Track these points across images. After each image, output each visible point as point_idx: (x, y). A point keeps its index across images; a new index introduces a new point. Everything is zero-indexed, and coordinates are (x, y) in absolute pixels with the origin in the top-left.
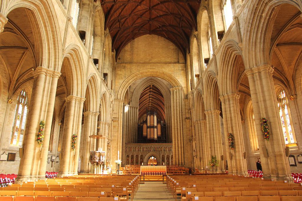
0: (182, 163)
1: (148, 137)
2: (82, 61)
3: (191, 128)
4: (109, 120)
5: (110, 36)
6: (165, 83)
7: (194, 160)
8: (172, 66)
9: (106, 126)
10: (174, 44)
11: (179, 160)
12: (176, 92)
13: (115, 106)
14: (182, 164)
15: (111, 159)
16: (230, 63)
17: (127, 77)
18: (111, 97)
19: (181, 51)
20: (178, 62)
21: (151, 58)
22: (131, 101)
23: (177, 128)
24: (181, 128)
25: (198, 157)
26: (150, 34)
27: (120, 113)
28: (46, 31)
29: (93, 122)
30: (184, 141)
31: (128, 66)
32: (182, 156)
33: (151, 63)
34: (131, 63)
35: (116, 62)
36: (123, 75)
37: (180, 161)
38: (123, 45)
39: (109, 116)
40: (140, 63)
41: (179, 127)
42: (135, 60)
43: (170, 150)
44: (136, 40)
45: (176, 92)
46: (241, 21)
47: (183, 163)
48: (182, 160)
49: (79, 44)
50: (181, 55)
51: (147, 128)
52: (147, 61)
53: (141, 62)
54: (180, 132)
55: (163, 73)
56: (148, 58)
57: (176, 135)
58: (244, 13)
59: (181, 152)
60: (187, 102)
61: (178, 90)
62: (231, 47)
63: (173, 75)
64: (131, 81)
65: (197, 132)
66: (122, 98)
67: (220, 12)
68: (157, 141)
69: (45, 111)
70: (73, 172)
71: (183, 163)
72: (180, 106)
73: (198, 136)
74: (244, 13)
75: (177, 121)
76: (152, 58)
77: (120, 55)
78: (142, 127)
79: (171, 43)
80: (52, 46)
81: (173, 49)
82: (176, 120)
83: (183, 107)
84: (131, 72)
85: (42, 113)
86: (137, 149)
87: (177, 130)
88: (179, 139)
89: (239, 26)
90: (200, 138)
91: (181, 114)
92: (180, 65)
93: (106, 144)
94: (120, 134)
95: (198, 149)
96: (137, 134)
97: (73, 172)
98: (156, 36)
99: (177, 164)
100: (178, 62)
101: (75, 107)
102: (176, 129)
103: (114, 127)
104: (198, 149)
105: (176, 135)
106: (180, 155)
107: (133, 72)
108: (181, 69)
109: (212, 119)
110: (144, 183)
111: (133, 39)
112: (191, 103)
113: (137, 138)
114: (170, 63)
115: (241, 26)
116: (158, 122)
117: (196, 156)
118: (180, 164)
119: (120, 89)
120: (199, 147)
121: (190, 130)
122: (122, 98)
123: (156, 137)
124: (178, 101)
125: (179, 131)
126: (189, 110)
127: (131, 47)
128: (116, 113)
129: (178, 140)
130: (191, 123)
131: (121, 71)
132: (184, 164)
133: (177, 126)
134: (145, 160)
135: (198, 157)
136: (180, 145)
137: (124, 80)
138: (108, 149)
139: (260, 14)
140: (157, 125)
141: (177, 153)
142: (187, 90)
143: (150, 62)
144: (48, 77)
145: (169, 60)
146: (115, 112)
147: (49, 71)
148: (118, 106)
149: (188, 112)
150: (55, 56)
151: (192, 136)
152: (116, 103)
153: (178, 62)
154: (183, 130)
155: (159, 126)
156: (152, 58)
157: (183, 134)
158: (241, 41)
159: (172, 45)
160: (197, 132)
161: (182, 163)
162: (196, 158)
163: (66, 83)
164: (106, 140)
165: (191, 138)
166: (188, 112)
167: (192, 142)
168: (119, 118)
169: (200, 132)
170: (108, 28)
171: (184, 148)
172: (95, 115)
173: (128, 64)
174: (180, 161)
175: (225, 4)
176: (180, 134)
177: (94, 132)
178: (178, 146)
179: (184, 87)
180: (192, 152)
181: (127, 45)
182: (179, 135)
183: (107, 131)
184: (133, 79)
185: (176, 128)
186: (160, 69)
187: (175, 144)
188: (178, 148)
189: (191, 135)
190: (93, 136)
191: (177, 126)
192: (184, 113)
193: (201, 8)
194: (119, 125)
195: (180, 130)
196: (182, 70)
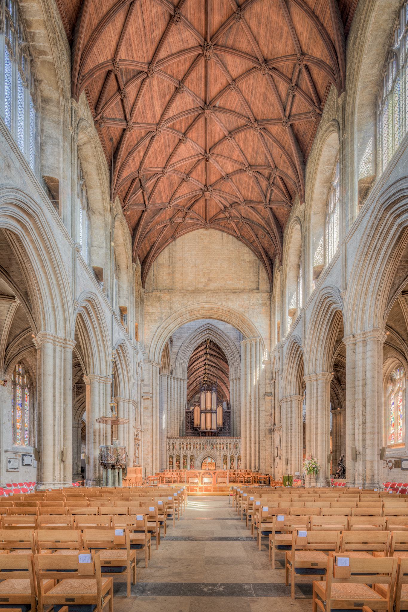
0: (255, 466)
7: (276, 462)
11: (250, 463)
15: (143, 460)
17: (164, 319)
27: (154, 384)
37: (253, 465)
48: (255, 463)
52: (201, 286)
56: (202, 280)
88: (253, 429)
106: (253, 455)
108: (261, 302)
117: (280, 456)
118: (253, 468)
119: (153, 340)
120: (287, 441)
121: (271, 415)
128: (148, 385)
132: (259, 469)
141: (248, 452)
146: (146, 382)
148: (151, 372)
174: (253, 465)
180: (273, 449)
188: (250, 444)
194: (154, 406)
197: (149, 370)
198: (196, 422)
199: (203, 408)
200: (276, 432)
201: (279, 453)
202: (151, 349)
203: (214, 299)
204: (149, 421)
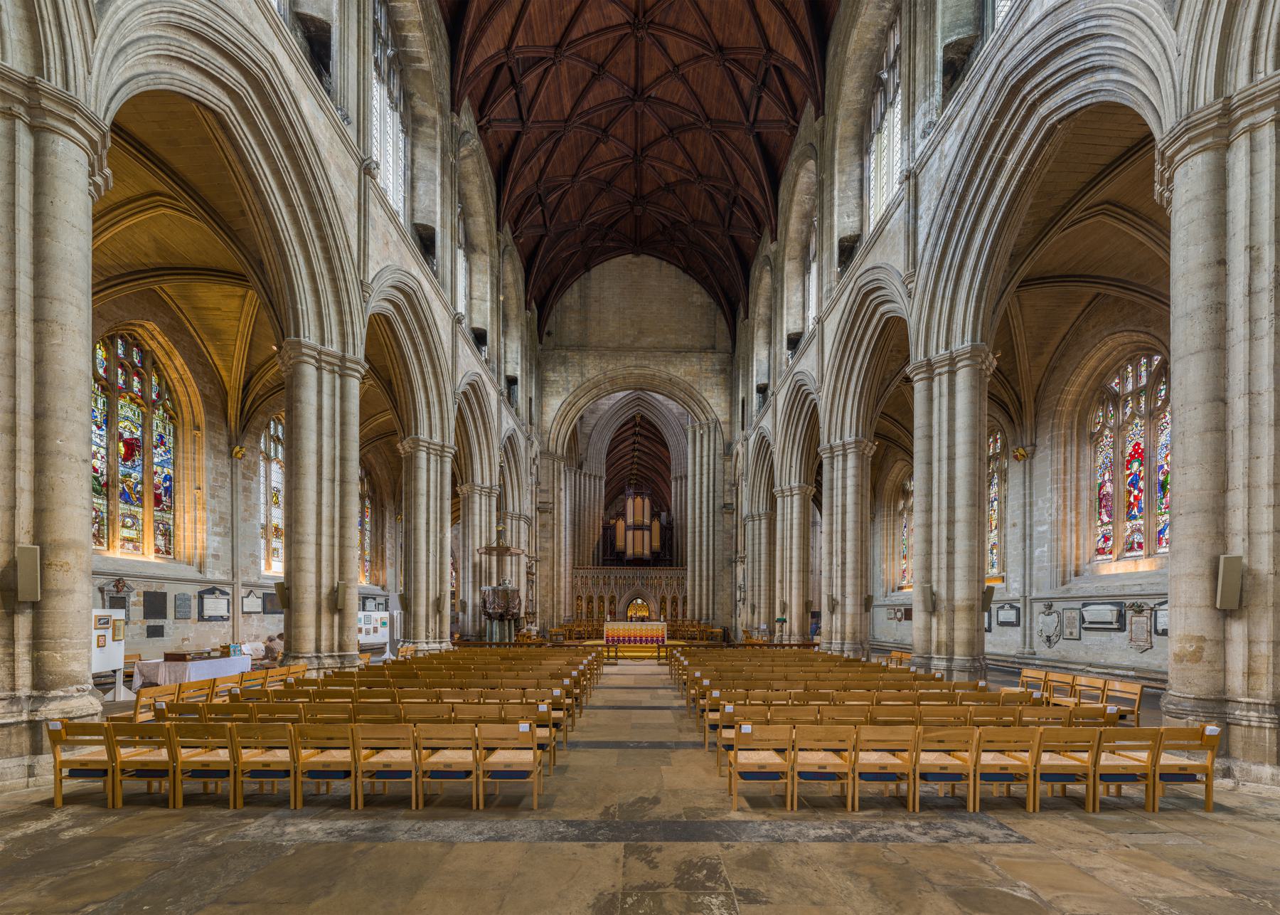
0: (708, 615)
1: (630, 552)
2: (435, 332)
4: (528, 508)
5: (516, 254)
9: (522, 523)
10: (703, 291)
11: (701, 609)
13: (543, 472)
14: (708, 619)
17: (571, 390)
18: (531, 446)
21: (639, 333)
23: (701, 532)
24: (711, 532)
25: (749, 603)
29: (483, 513)
32: (708, 599)
33: (637, 349)
35: (541, 342)
37: (704, 612)
38: (558, 290)
39: (529, 497)
40: (608, 348)
41: (704, 529)
43: (682, 585)
47: (711, 616)
48: (708, 609)
49: (415, 271)
50: (722, 326)
52: (628, 341)
53: (610, 344)
55: (670, 380)
57: (697, 548)
60: (728, 464)
63: (697, 387)
64: (582, 401)
65: (750, 543)
66: (559, 451)
68: (649, 561)
69: (333, 481)
71: (711, 616)
72: (711, 475)
73: (750, 553)
75: (701, 513)
76: (641, 332)
77: (549, 321)
78: (614, 527)
79: (696, 287)
81: (701, 306)
82: (697, 511)
83: (719, 476)
84: (582, 375)
85: (326, 485)
86: (601, 582)
87: (701, 536)
91: (711, 495)
92: (716, 356)
93: (523, 570)
96: (601, 543)
98: (653, 259)
99: (697, 616)
100: (713, 348)
101: (428, 470)
102: (697, 534)
103: (543, 526)
104: (749, 584)
105: (697, 548)
106: (704, 597)
107: (587, 375)
108: (718, 367)
109: (792, 507)
110: (616, 664)
112: (739, 465)
113: (601, 554)
118: (704, 617)
122: (559, 451)
123: (647, 552)
124: (705, 459)
125: (704, 538)
126: (734, 485)
127: (580, 297)
128: (547, 491)
129: (701, 561)
133: (701, 526)
134: (620, 607)
135: (749, 603)
136: (705, 573)
137: (563, 398)
138: (528, 581)
140: (651, 522)
141: (697, 593)
143: (636, 345)
144: (326, 377)
145: (685, 341)
147: (328, 355)
149: (730, 491)
150: (339, 302)
151: (737, 552)
152: (545, 461)
153: (713, 348)
155: (656, 525)
156: (641, 332)
157: (714, 545)
159: (696, 293)
161: (708, 615)
163: (396, 400)
164: (524, 560)
166: (730, 491)
170: (507, 224)
171: (714, 580)
172: (489, 496)
173: (573, 351)
177: (490, 538)
178: (701, 576)
179: (725, 423)
182: (704, 548)
183: (524, 537)
184: (589, 396)
185: (697, 530)
186: (662, 368)
187: (694, 571)
188: (701, 580)
190: (489, 550)
191: (701, 526)
192: (719, 493)
195: (708, 535)
196: (723, 371)
198: (620, 543)
199: (630, 521)
204: (548, 545)
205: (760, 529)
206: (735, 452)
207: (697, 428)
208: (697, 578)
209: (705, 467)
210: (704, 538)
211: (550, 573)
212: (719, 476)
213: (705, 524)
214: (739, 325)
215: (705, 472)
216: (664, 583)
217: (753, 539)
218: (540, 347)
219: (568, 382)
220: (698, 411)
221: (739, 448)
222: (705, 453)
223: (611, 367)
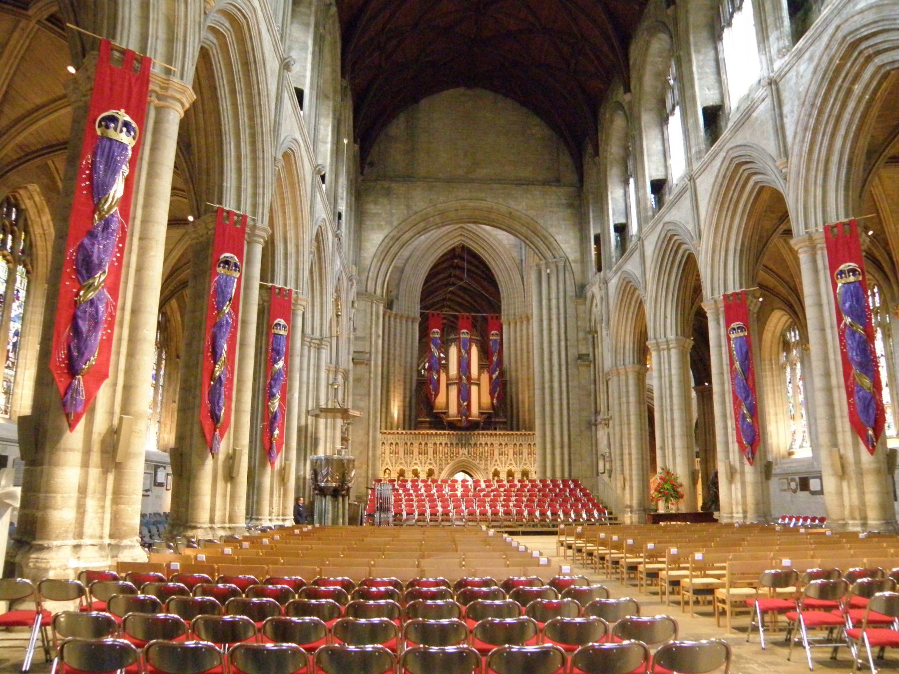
3: (593, 386)
6: (505, 242)
8: (537, 191)
12: (549, 276)
16: (741, 206)
17: (395, 224)
19: (567, 143)
20: (558, 181)
22: (397, 298)
23: (551, 388)
26: (469, 87)
28: (235, 104)
30: (572, 425)
31: (399, 188)
33: (472, 181)
34: (408, 178)
35: (362, 173)
36: (384, 215)
41: (556, 385)
42: (422, 171)
44: (424, 103)
45: (549, 276)
46: (786, 95)
50: (566, 159)
51: (448, 385)
52: (460, 172)
53: (441, 175)
54: (561, 399)
58: (798, 73)
59: (562, 460)
60: (581, 308)
61: (555, 270)
62: (746, 163)
63: (541, 222)
66: (379, 291)
67: (711, 46)
70: (281, 517)
72: (562, 321)
73: (617, 414)
74: (798, 73)
79: (537, 120)
80: (246, 149)
82: (546, 363)
83: (571, 323)
84: (408, 207)
87: (552, 394)
89: (780, 106)
90: (626, 418)
91: (563, 343)
94: (375, 403)
95: (616, 451)
97: (281, 517)
98: (488, 92)
102: (547, 391)
103: (357, 380)
104: (616, 451)
108: (564, 202)
111: (416, 100)
114: (531, 183)
115: (786, 109)
116: (481, 368)
117: (610, 471)
119: (375, 260)
122: (379, 291)
124: (554, 302)
126: (589, 332)
128: (362, 339)
130: (592, 372)
131: (376, 203)
133: (551, 381)
137: (386, 232)
139: (846, 85)
141: (549, 464)
142: (584, 272)
143: (470, 176)
145: (526, 173)
148: (369, 315)
152: (362, 303)
154: (568, 392)
157: (568, 404)
158: (785, 152)
160: (614, 402)
162: (610, 477)
165: (593, 419)
166: (585, 339)
167: (596, 431)
168: (370, 353)
169: (624, 399)
171: (570, 447)
173: (398, 182)
175: (729, 24)
176: (561, 405)
178: (553, 442)
179: (575, 262)
180: (595, 460)
181: (395, 121)
182: (557, 408)
185: (547, 385)
186: (501, 200)
188: (553, 448)
189: (593, 410)
191: (551, 381)
193: (646, 24)
194: (372, 376)
196: (570, 206)
197: (365, 311)
200: (599, 427)
201: (608, 466)
202: (371, 274)
203: (483, 195)
205: (627, 385)
206: (589, 295)
207: (543, 267)
208: (548, 446)
209: (554, 311)
210: (556, 396)
211: (365, 440)
212: (571, 323)
213: (556, 379)
214: (587, 159)
215: (554, 317)
216: (496, 452)
217: (620, 398)
218: (361, 178)
219: (392, 215)
220: (543, 247)
221: (595, 290)
222: (553, 295)
223: (441, 199)
